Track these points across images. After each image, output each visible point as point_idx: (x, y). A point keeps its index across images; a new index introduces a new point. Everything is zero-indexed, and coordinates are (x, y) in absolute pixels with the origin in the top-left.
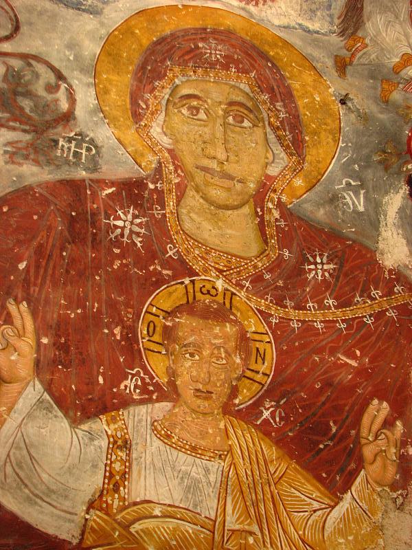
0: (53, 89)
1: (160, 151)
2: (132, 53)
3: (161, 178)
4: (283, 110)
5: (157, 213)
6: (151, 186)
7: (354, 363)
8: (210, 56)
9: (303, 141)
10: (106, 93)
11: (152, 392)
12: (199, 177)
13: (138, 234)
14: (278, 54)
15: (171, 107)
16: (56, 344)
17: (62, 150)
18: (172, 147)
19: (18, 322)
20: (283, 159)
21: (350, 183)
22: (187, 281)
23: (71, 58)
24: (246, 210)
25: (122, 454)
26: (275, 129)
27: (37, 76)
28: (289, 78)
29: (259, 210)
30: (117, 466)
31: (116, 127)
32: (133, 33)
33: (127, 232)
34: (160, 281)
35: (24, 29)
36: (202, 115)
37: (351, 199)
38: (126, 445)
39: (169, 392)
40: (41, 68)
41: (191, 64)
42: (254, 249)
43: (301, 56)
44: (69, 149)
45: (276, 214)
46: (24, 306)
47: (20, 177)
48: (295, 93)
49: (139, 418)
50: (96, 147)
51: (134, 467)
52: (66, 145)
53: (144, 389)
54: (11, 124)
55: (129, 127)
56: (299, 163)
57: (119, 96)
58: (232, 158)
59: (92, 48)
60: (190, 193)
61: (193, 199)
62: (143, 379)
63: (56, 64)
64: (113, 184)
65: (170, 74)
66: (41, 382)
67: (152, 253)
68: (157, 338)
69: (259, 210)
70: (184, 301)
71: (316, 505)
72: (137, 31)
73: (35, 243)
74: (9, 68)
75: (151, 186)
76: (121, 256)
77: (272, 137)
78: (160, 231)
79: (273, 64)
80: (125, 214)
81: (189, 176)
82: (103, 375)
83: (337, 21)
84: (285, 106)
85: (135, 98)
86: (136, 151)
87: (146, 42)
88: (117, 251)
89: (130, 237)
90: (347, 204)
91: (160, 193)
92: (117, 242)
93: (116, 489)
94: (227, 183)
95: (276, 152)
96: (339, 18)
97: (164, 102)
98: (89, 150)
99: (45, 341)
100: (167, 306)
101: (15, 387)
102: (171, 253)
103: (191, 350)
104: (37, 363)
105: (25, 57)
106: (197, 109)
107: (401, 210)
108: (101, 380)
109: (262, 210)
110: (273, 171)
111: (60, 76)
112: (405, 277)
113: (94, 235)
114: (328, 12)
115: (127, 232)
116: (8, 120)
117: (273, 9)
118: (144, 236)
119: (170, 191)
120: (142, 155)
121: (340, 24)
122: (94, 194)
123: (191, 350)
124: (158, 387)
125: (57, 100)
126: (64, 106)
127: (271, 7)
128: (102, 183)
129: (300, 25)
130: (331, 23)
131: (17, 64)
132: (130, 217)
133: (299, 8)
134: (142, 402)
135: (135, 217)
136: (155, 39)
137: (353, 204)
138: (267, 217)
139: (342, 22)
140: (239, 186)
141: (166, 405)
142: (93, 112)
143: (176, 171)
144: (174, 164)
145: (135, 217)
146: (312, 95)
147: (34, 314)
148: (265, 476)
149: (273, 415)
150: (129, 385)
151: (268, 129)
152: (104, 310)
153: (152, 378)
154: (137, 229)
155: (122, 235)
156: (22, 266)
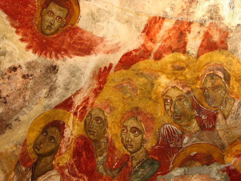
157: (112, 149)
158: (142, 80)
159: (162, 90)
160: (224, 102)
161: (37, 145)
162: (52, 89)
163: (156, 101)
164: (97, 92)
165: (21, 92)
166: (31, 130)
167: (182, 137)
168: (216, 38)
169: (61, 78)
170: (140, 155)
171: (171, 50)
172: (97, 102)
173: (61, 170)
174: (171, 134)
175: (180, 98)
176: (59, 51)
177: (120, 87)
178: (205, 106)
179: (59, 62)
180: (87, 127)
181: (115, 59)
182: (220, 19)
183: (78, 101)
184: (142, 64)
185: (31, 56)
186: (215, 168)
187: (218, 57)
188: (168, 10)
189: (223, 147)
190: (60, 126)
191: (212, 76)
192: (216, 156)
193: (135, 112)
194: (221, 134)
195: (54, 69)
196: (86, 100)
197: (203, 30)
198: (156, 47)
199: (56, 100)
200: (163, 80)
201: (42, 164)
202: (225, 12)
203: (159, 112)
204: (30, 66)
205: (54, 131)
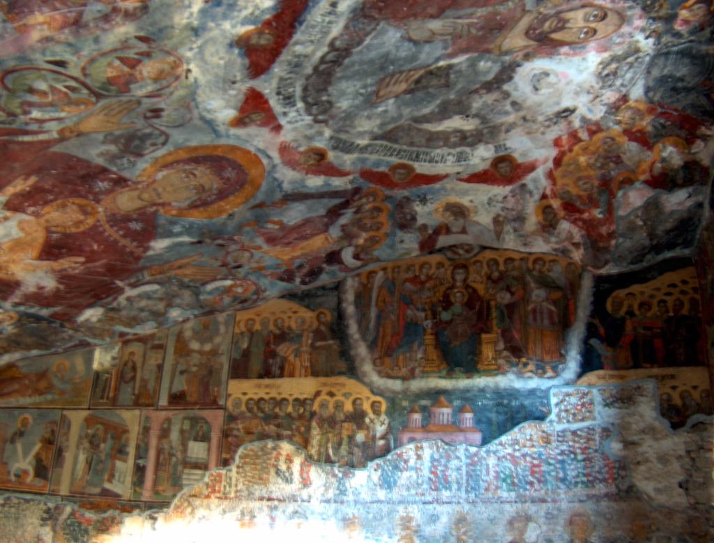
83: (296, 191)
110: (174, 204)
157: (580, 197)
158: (572, 167)
159: (584, 164)
160: (619, 147)
161: (545, 219)
162: (531, 193)
163: (586, 170)
164: (554, 184)
165: (517, 202)
166: (537, 216)
167: (609, 173)
168: (594, 128)
169: (531, 186)
170: (595, 190)
171: (575, 144)
172: (558, 187)
173: (564, 218)
174: (603, 175)
175: (596, 160)
176: (519, 178)
177: (564, 176)
178: (610, 155)
179: (524, 181)
180: (562, 198)
181: (550, 164)
182: (589, 120)
183: (548, 192)
184: (566, 159)
185: (508, 188)
186: (637, 185)
187: (600, 136)
188: (560, 133)
189: (633, 172)
190: (550, 207)
191: (605, 143)
192: (632, 177)
193: (579, 179)
194: (628, 163)
195: (524, 185)
196: (552, 190)
197: (585, 129)
198: (566, 148)
199: (537, 197)
200: (582, 159)
201: (553, 222)
202: (589, 116)
203: (592, 173)
204: (511, 191)
205: (548, 210)
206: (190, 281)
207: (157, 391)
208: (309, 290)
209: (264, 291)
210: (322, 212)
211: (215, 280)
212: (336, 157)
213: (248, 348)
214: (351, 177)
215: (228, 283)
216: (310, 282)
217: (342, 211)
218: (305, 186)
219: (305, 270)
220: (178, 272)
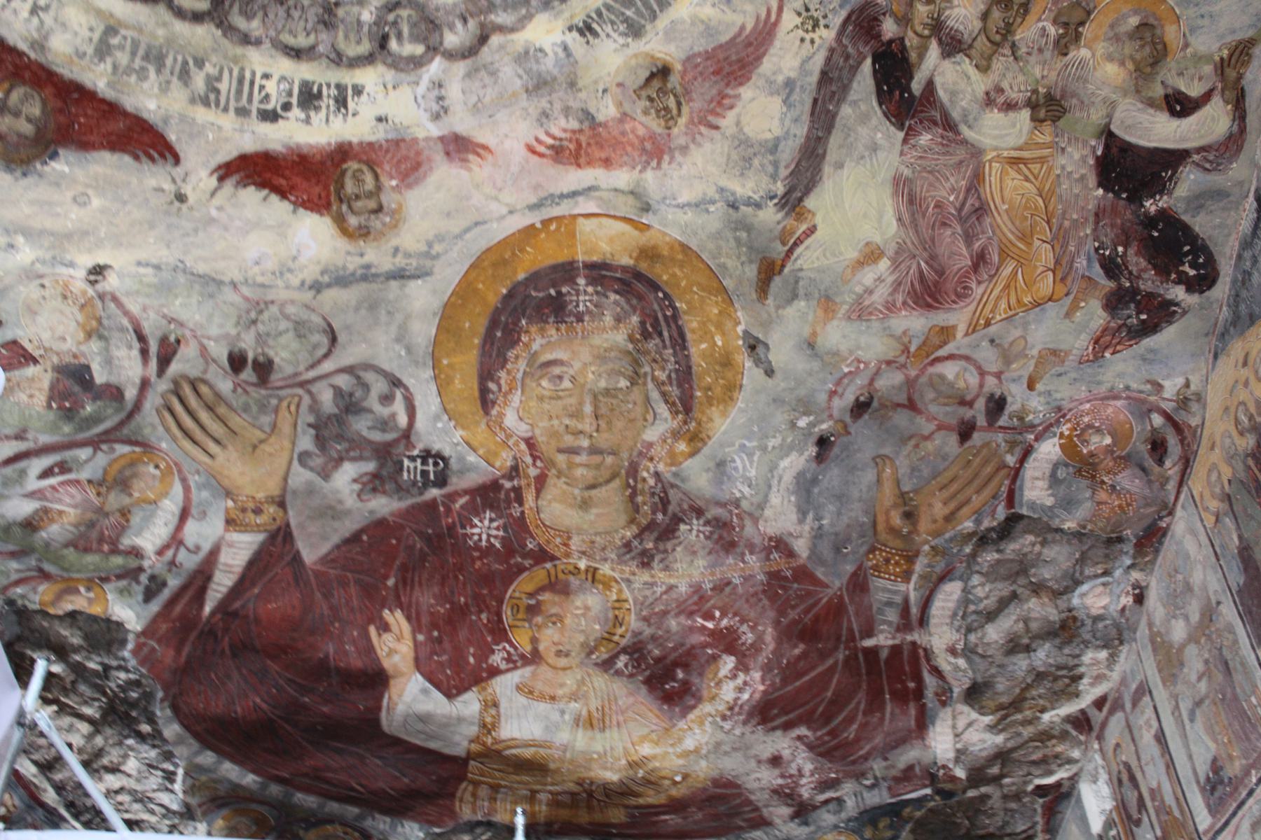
0: (387, 399)
1: (516, 444)
2: (474, 324)
3: (518, 475)
4: (672, 359)
5: (516, 511)
6: (508, 485)
7: (710, 625)
8: (578, 305)
9: (692, 397)
10: (448, 384)
11: (514, 662)
12: (561, 459)
13: (496, 537)
14: (674, 275)
15: (528, 381)
16: (430, 638)
17: (409, 471)
18: (530, 434)
19: (394, 627)
20: (666, 420)
21: (744, 445)
22: (548, 565)
23: (403, 353)
24: (616, 483)
25: (493, 712)
26: (659, 384)
27: (366, 387)
28: (685, 313)
29: (631, 481)
30: (489, 720)
31: (463, 428)
32: (476, 291)
33: (484, 537)
34: (522, 569)
35: (342, 338)
36: (566, 384)
37: (742, 460)
38: (496, 705)
39: (534, 658)
40: (369, 377)
41: (551, 320)
42: (623, 519)
43: (708, 271)
44: (416, 468)
45: (652, 482)
46: (398, 613)
47: (371, 512)
48: (689, 336)
49: (504, 686)
50: (443, 459)
51: (503, 719)
52: (412, 465)
53: (509, 659)
54: (352, 454)
55: (477, 423)
56: (685, 423)
57: (465, 382)
58: (603, 424)
59: (424, 331)
60: (551, 481)
61: (555, 487)
62: (508, 653)
63: (386, 366)
64: (466, 492)
65: (524, 338)
66: (422, 674)
67: (511, 548)
68: (520, 616)
69: (631, 481)
70: (546, 581)
71: (654, 727)
72: (480, 286)
73: (398, 563)
74: (338, 392)
75: (508, 485)
76: (480, 558)
77: (655, 395)
78: (519, 527)
79: (665, 294)
80: (481, 521)
81: (551, 463)
82: (474, 656)
83: (784, 172)
84: (675, 354)
85: (486, 375)
86: (489, 451)
87: (493, 299)
88: (476, 554)
89: (488, 541)
90: (736, 469)
91: (518, 491)
92: (477, 547)
93: (489, 732)
94: (597, 459)
95: (659, 411)
96: (787, 167)
97: (519, 375)
98: (436, 464)
99: (421, 637)
100: (530, 588)
101: (402, 680)
102: (530, 546)
103: (554, 619)
104: (417, 660)
105: (349, 370)
106: (560, 378)
107: (800, 476)
108: (472, 660)
109: (636, 481)
111: (396, 383)
112: (786, 544)
113: (452, 545)
114: (771, 158)
115: (484, 537)
116: (347, 451)
117: (685, 167)
118: (503, 538)
119: (529, 485)
120: (496, 454)
121: (786, 178)
122: (449, 510)
123: (554, 619)
124: (523, 656)
125: (393, 416)
126: (403, 420)
127: (680, 165)
128: (452, 497)
129: (722, 190)
130: (774, 177)
131: (343, 381)
132: (486, 522)
133: (725, 160)
134: (508, 670)
135: (491, 520)
136: (504, 291)
137: (744, 467)
138: (639, 486)
139: (791, 174)
140: (609, 460)
141: (527, 671)
142: (437, 418)
143: (534, 464)
144: (531, 455)
145: (491, 520)
146: (713, 338)
147: (409, 618)
148: (614, 707)
149: (626, 666)
150: (497, 659)
151: (650, 385)
152: (470, 602)
153: (516, 648)
154: (494, 532)
155: (480, 540)
156: (391, 582)
206: (978, 522)
207: (1182, 799)
208: (1234, 282)
209: (1159, 387)
210: (886, 135)
211: (1016, 473)
212: (669, 35)
213: (1240, 537)
214: (789, 20)
215: (1049, 450)
216: (1211, 262)
217: (917, 86)
218: (773, 147)
219: (1136, 261)
220: (924, 525)
